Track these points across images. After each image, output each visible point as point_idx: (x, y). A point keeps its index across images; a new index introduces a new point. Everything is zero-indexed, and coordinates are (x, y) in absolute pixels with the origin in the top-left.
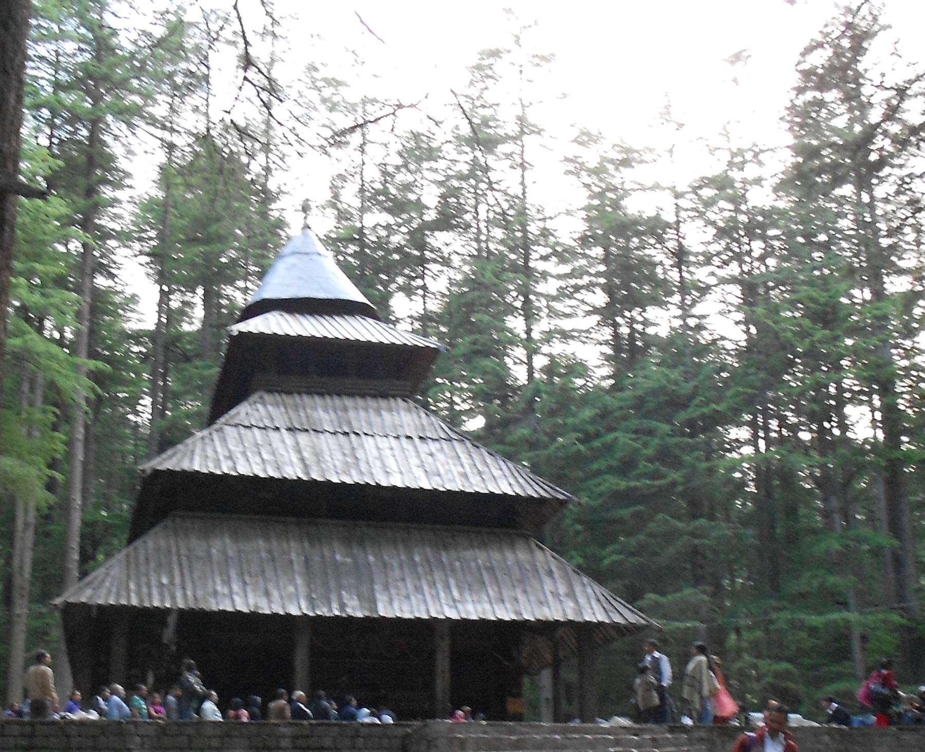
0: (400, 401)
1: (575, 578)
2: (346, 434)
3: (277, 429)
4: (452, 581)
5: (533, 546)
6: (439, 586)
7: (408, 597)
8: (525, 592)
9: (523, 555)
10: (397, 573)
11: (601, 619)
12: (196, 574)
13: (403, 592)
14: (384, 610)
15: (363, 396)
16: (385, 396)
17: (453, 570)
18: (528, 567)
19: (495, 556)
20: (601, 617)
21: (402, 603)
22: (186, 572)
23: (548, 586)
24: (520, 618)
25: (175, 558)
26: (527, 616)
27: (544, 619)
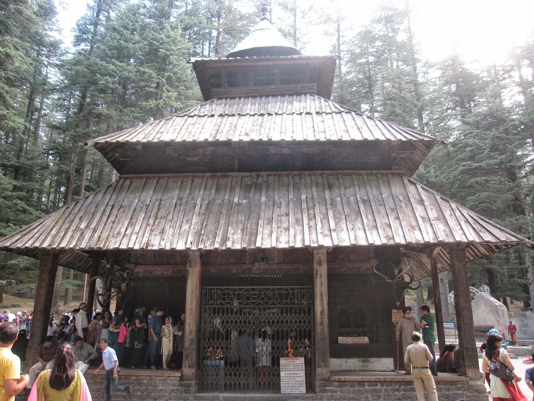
0: (308, 96)
1: (444, 205)
2: (262, 115)
3: (213, 116)
4: (330, 213)
5: (406, 181)
6: (318, 218)
7: (287, 229)
8: (398, 218)
9: (397, 190)
10: (283, 210)
11: (471, 238)
12: (112, 218)
13: (285, 225)
14: (266, 240)
15: (283, 95)
16: (299, 94)
17: (333, 204)
18: (401, 198)
19: (373, 192)
20: (472, 237)
21: (275, 236)
22: (105, 218)
23: (419, 211)
24: (391, 242)
25: (102, 208)
26: (400, 240)
27: (414, 241)
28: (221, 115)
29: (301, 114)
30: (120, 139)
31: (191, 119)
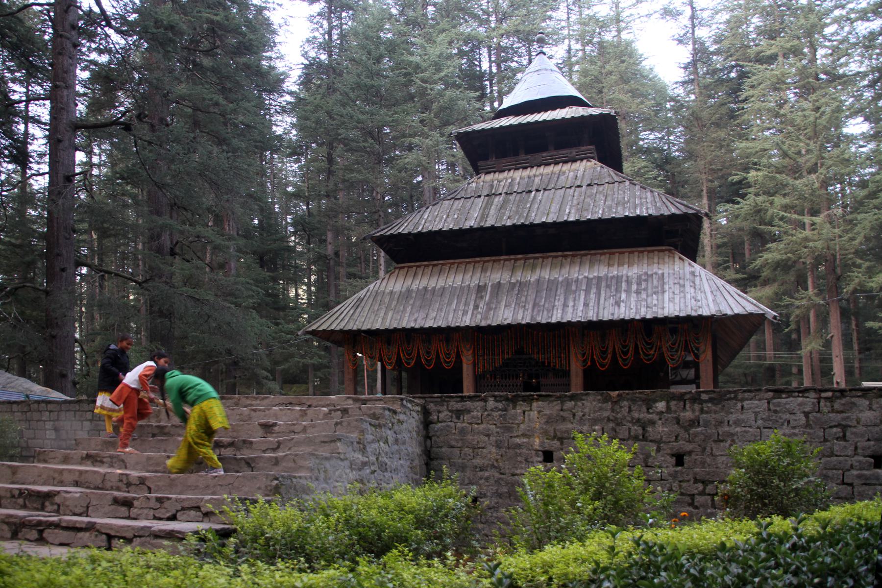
28: (488, 195)
29: (571, 187)
30: (392, 232)
31: (457, 202)
